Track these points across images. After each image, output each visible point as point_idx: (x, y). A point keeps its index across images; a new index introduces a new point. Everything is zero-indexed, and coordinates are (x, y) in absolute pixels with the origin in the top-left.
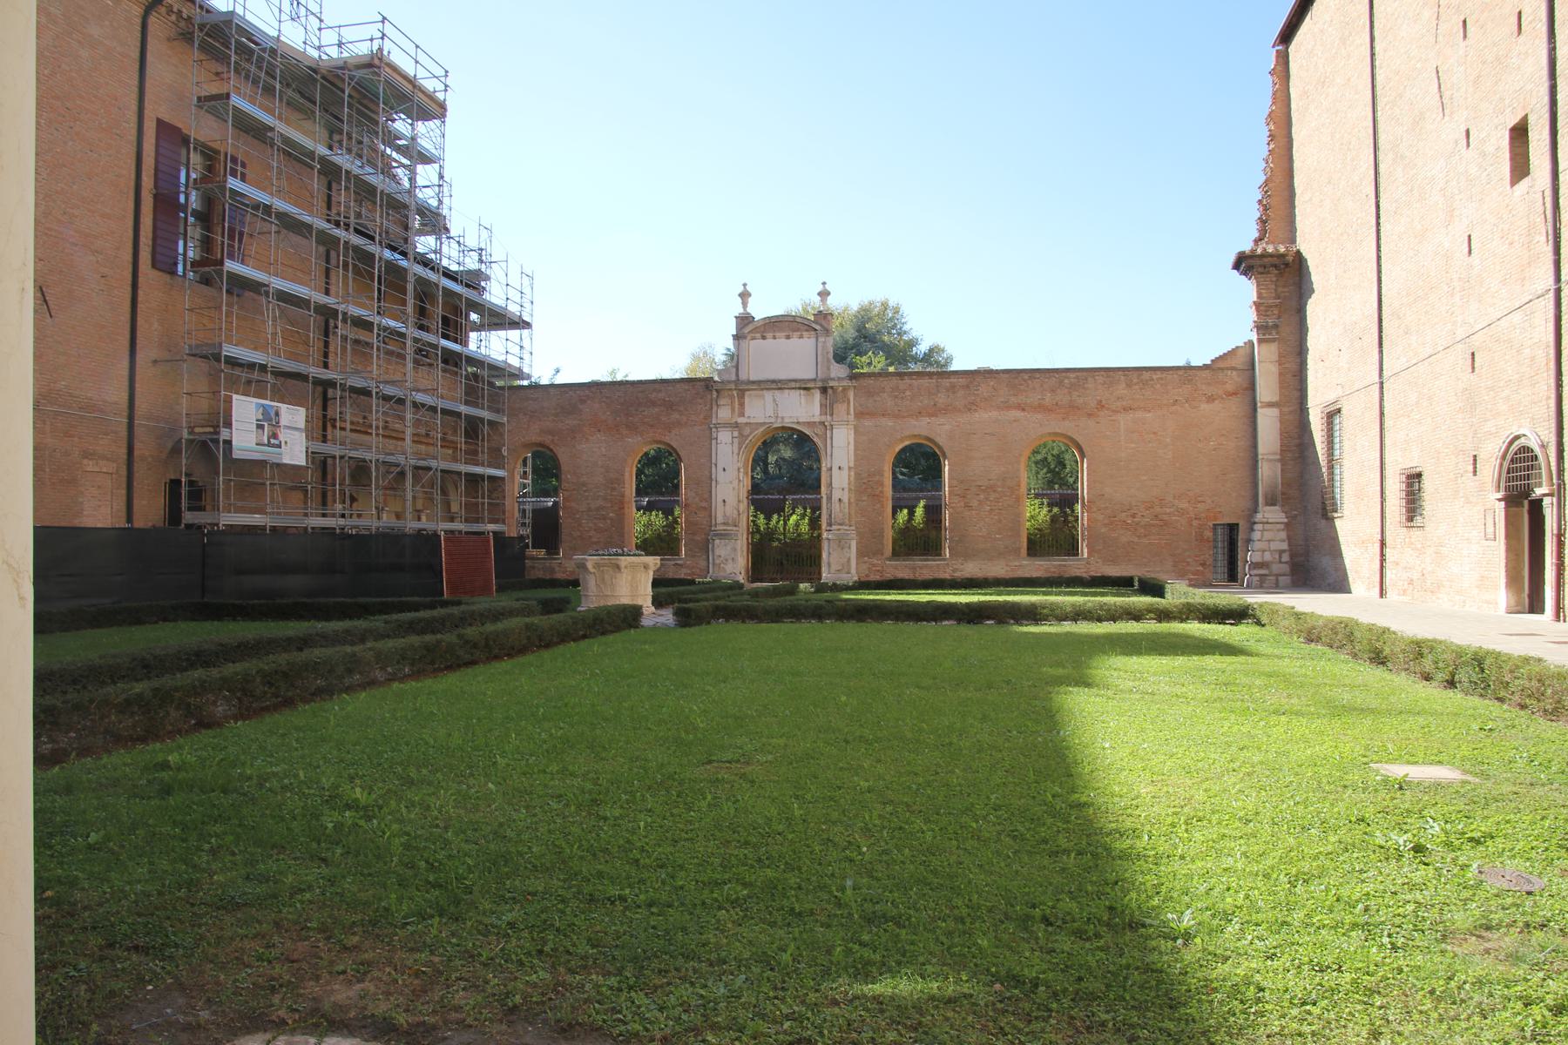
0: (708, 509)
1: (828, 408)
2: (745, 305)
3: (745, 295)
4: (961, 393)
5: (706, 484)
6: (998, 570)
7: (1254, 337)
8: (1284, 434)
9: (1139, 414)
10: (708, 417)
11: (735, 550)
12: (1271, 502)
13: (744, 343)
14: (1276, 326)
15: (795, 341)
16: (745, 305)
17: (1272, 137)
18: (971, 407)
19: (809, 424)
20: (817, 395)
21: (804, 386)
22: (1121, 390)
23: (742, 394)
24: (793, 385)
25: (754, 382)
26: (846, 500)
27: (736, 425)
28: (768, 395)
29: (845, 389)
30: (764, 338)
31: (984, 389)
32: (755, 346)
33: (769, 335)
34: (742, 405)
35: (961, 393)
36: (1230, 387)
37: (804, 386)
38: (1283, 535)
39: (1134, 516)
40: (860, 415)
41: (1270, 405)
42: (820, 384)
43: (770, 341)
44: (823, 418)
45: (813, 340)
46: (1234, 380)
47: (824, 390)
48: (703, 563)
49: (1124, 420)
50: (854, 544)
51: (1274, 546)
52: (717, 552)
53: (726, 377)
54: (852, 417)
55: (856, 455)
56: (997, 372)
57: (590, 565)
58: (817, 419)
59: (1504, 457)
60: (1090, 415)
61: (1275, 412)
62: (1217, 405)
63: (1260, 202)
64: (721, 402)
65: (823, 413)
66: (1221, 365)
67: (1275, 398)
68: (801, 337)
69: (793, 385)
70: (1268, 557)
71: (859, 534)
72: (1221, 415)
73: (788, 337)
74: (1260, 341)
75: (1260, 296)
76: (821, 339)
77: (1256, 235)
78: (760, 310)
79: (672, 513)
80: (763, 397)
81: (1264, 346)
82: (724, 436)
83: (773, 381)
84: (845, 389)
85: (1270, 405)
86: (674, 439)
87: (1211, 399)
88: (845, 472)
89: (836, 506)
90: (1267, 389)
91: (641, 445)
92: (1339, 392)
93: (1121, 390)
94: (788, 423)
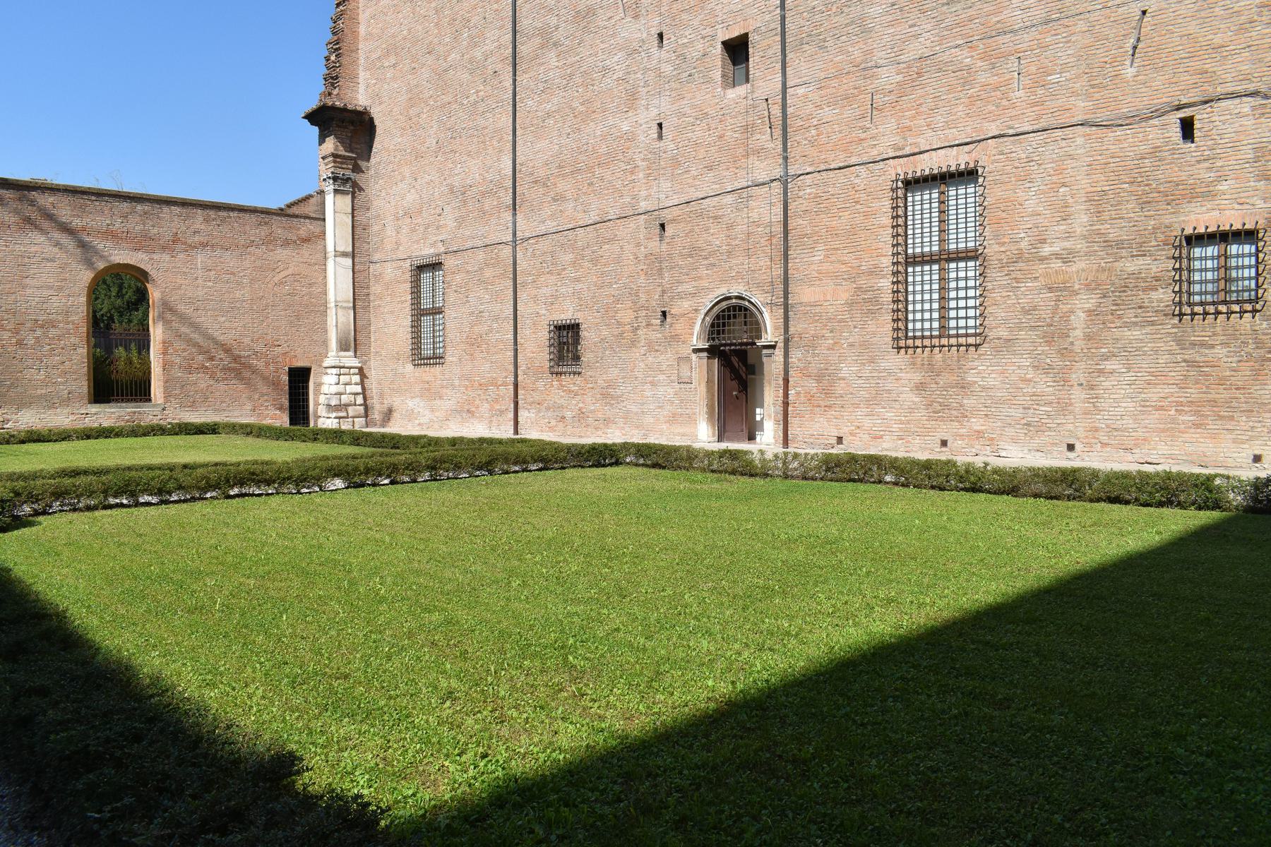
6: (61, 419)
51: (349, 389)
70: (345, 399)
74: (336, 191)
81: (339, 197)
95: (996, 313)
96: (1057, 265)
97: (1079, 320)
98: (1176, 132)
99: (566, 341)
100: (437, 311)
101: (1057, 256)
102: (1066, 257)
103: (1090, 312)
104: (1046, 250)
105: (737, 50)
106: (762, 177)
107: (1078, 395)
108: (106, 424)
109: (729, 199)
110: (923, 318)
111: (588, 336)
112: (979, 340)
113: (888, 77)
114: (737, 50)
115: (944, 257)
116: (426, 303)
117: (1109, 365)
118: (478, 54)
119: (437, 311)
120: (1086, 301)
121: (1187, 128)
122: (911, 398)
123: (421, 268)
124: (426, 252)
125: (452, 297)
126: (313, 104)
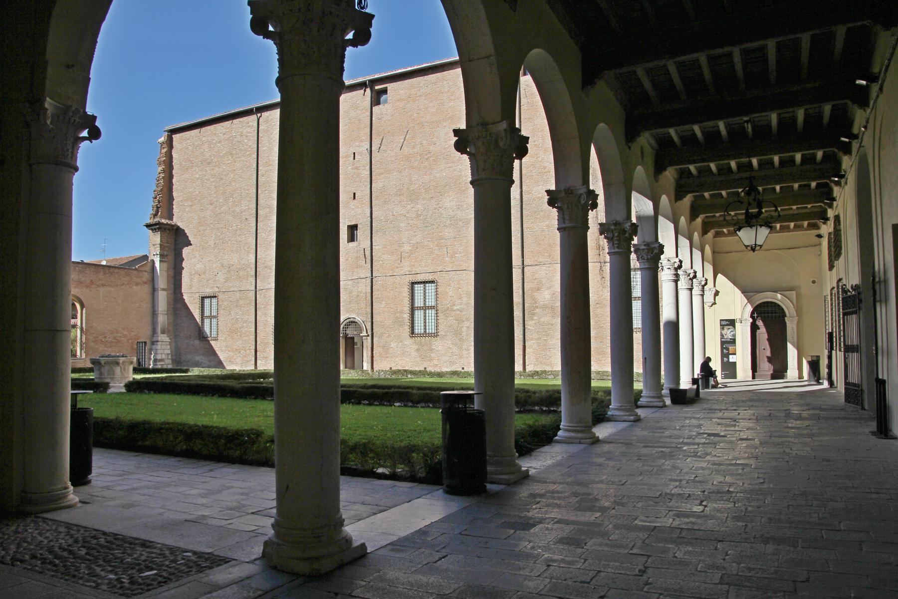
9: (109, 289)
12: (163, 332)
17: (164, 171)
36: (144, 279)
38: (169, 347)
41: (163, 290)
49: (102, 290)
61: (165, 293)
62: (139, 287)
63: (156, 198)
70: (164, 357)
74: (161, 261)
85: (163, 290)
87: (137, 284)
92: (217, 290)
95: (441, 327)
102: (461, 310)
104: (455, 308)
106: (363, 276)
109: (350, 283)
110: (419, 328)
112: (435, 335)
113: (407, 248)
115: (425, 308)
116: (207, 313)
118: (237, 209)
122: (414, 354)
124: (208, 291)
125: (221, 312)
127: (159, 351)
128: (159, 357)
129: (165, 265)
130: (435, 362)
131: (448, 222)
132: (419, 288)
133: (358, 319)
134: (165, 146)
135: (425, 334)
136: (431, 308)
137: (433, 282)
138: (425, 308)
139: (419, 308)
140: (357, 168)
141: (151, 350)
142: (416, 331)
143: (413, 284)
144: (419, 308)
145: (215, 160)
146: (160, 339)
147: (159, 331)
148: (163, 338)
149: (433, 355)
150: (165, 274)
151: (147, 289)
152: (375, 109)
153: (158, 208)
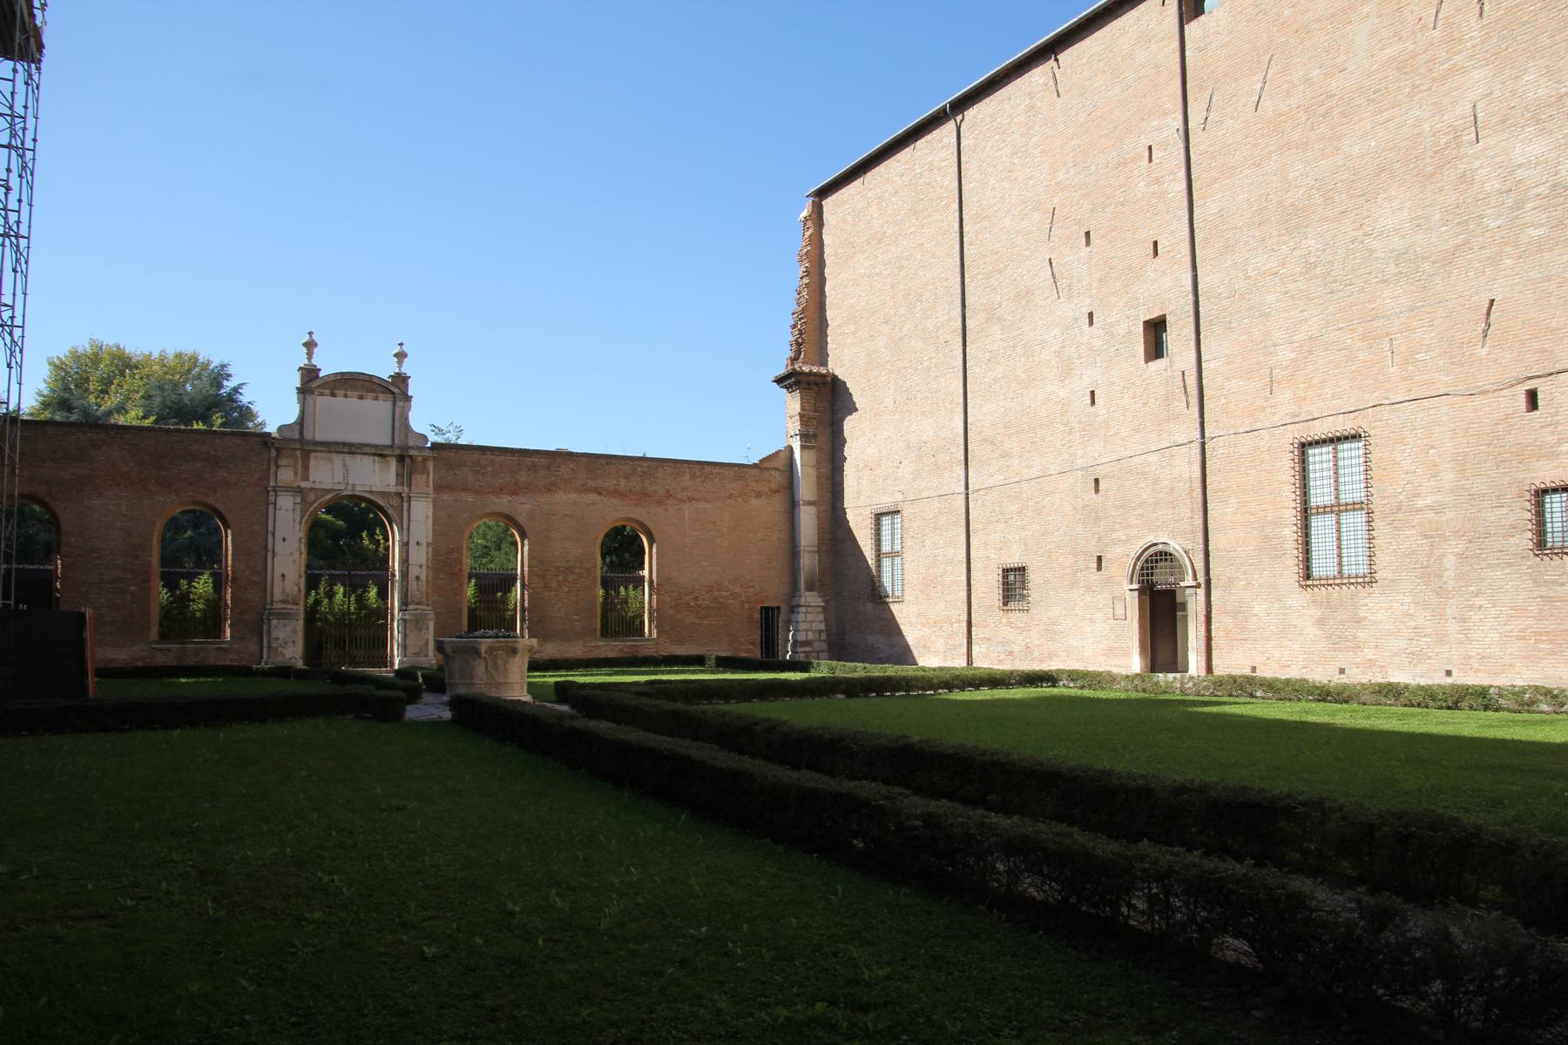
0: (263, 586)
1: (405, 477)
2: (310, 355)
3: (310, 345)
4: (542, 473)
5: (257, 553)
6: (576, 651)
7: (796, 445)
8: (821, 530)
9: (702, 505)
10: (265, 477)
11: (295, 631)
12: (810, 588)
13: (310, 398)
14: (815, 436)
15: (368, 403)
16: (310, 355)
17: (808, 273)
18: (551, 488)
19: (384, 494)
20: (393, 463)
21: (379, 452)
22: (686, 481)
23: (306, 455)
24: (368, 450)
25: (322, 443)
26: (423, 577)
27: (299, 491)
28: (338, 460)
29: (425, 459)
30: (333, 395)
31: (565, 470)
32: (322, 402)
33: (340, 393)
34: (306, 467)
35: (542, 473)
36: (774, 485)
37: (379, 452)
38: (821, 617)
39: (696, 599)
40: (439, 488)
41: (810, 503)
42: (397, 452)
43: (340, 400)
44: (399, 489)
45: (389, 404)
46: (777, 479)
47: (401, 459)
48: (253, 647)
49: (688, 510)
50: (431, 625)
52: (274, 634)
53: (288, 434)
54: (431, 490)
55: (434, 530)
56: (577, 454)
57: (483, 649)
58: (392, 489)
59: (1138, 559)
60: (659, 503)
61: (812, 510)
62: (763, 501)
63: (794, 326)
64: (282, 462)
65: (400, 482)
66: (766, 465)
67: (814, 498)
68: (376, 399)
69: (368, 450)
70: (811, 636)
71: (436, 614)
72: (767, 509)
73: (361, 397)
74: (803, 447)
75: (802, 408)
76: (400, 404)
77: (791, 354)
78: (328, 365)
79: (177, 586)
80: (330, 460)
82: (285, 502)
83: (344, 444)
84: (425, 459)
85: (810, 503)
86: (219, 501)
87: (759, 495)
88: (424, 548)
89: (413, 585)
90: (806, 488)
91: (172, 505)
92: (899, 497)
93: (686, 481)
94: (359, 490)
95: (1382, 559)
96: (1430, 515)
97: (1450, 561)
98: (1522, 400)
99: (1013, 584)
100: (893, 554)
101: (1429, 508)
102: (1437, 509)
103: (1460, 556)
104: (1420, 503)
105: (1156, 329)
106: (1182, 439)
107: (1453, 628)
108: (610, 655)
109: (1153, 458)
110: (1323, 564)
111: (1033, 577)
112: (1369, 580)
113: (1284, 355)
114: (1156, 329)
115: (1338, 509)
116: (886, 548)
117: (1477, 602)
118: (930, 324)
119: (893, 554)
120: (1455, 546)
121: (1532, 399)
122: (1312, 631)
123: (878, 517)
124: (886, 502)
125: (909, 542)
126: (782, 370)
127: (802, 626)
128: (801, 637)
129: (812, 454)
130: (1369, 654)
131: (1392, 269)
132: (1319, 456)
133: (1175, 546)
134: (809, 224)
135: (1341, 579)
136: (1355, 506)
137: (1355, 437)
138: (1338, 509)
139: (1324, 510)
140: (1157, 181)
141: (789, 622)
142: (1316, 572)
143: (1304, 446)
144: (1324, 510)
145: (890, 231)
146: (803, 601)
147: (802, 586)
148: (811, 599)
149: (1361, 635)
150: (812, 472)
151: (777, 504)
152: (1192, 29)
153: (799, 344)
